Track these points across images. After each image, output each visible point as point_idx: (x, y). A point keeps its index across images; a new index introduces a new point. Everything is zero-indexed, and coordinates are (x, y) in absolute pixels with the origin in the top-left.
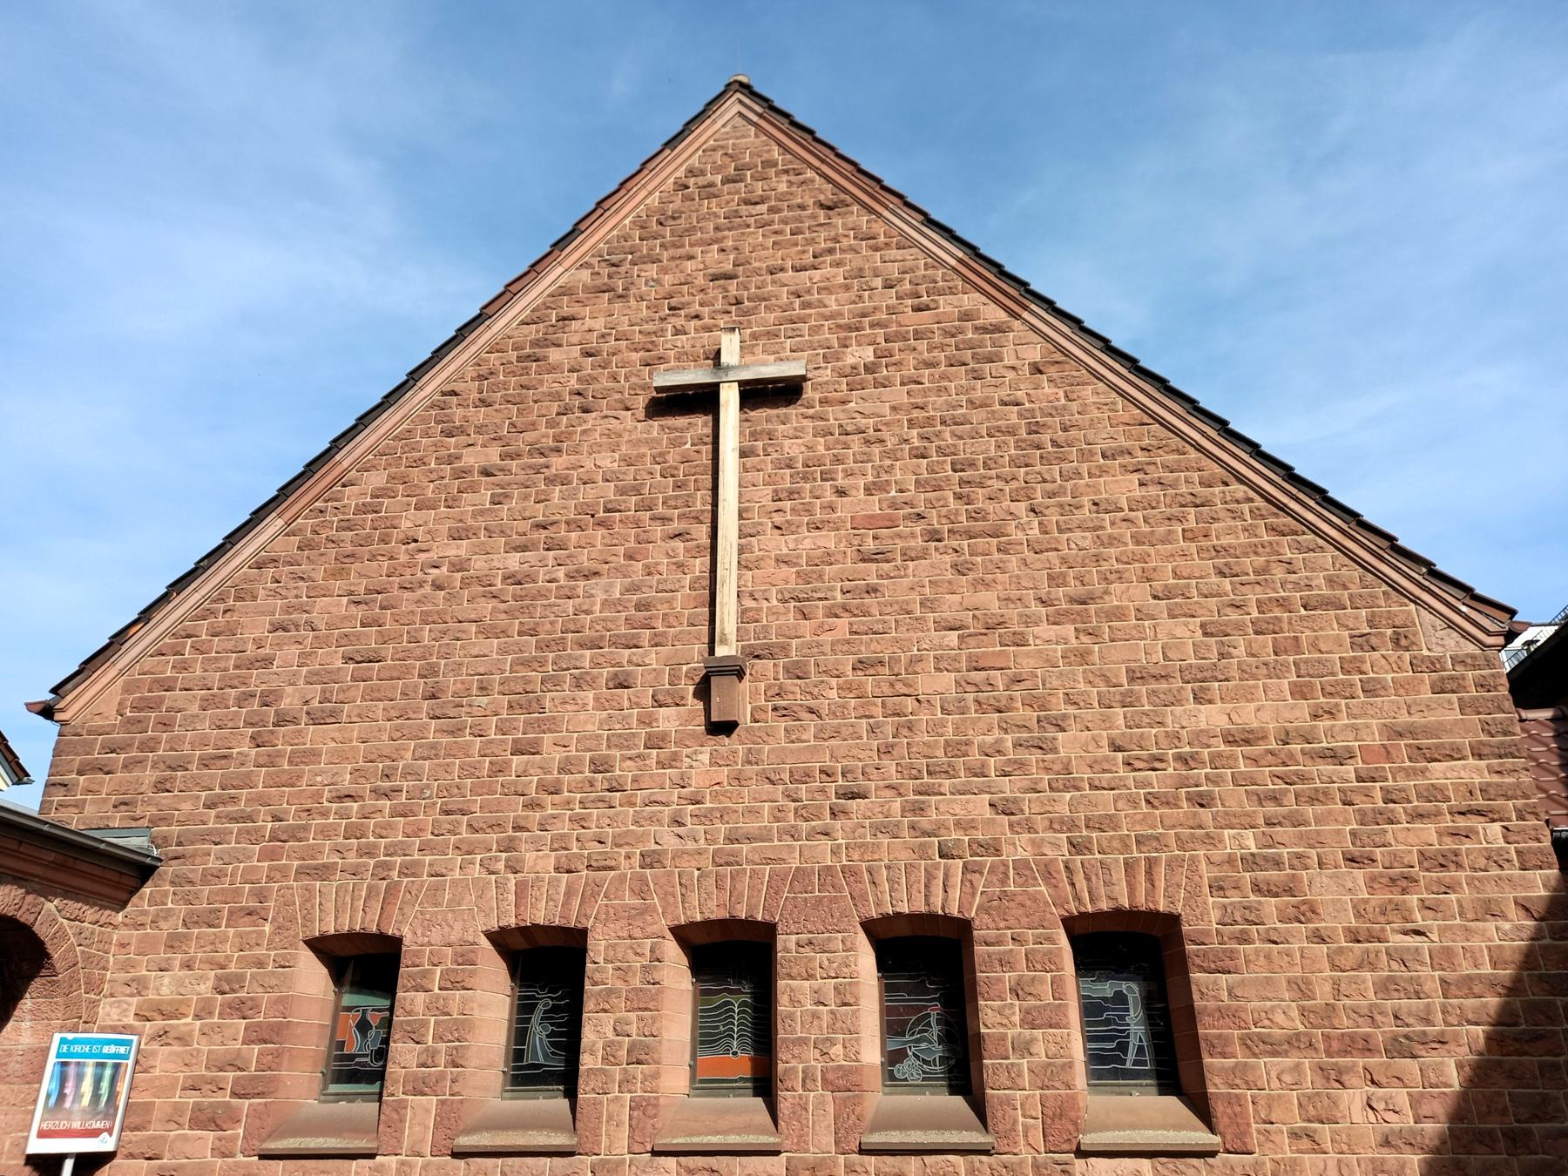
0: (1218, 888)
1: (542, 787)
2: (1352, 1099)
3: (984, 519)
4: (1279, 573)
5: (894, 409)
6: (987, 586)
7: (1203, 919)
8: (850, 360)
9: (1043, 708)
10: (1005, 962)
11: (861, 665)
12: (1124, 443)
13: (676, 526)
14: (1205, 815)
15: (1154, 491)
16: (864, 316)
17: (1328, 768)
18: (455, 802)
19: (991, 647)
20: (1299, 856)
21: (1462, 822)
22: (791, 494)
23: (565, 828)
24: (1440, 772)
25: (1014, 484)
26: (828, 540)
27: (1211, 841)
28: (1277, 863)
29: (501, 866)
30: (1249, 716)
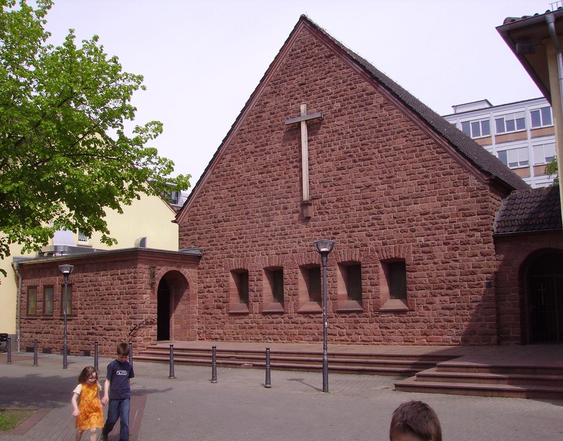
0: (414, 252)
1: (271, 235)
2: (437, 299)
3: (367, 155)
4: (438, 166)
5: (346, 122)
6: (368, 175)
7: (410, 259)
8: (335, 108)
9: (379, 208)
10: (367, 272)
11: (338, 200)
12: (403, 128)
13: (295, 164)
14: (414, 234)
15: (409, 142)
16: (338, 93)
17: (443, 220)
18: (254, 239)
19: (367, 193)
20: (433, 243)
21: (472, 233)
22: (321, 152)
23: (276, 245)
24: (469, 220)
25: (375, 144)
26: (330, 164)
27: (414, 241)
28: (428, 246)
29: (265, 254)
30: (427, 207)
